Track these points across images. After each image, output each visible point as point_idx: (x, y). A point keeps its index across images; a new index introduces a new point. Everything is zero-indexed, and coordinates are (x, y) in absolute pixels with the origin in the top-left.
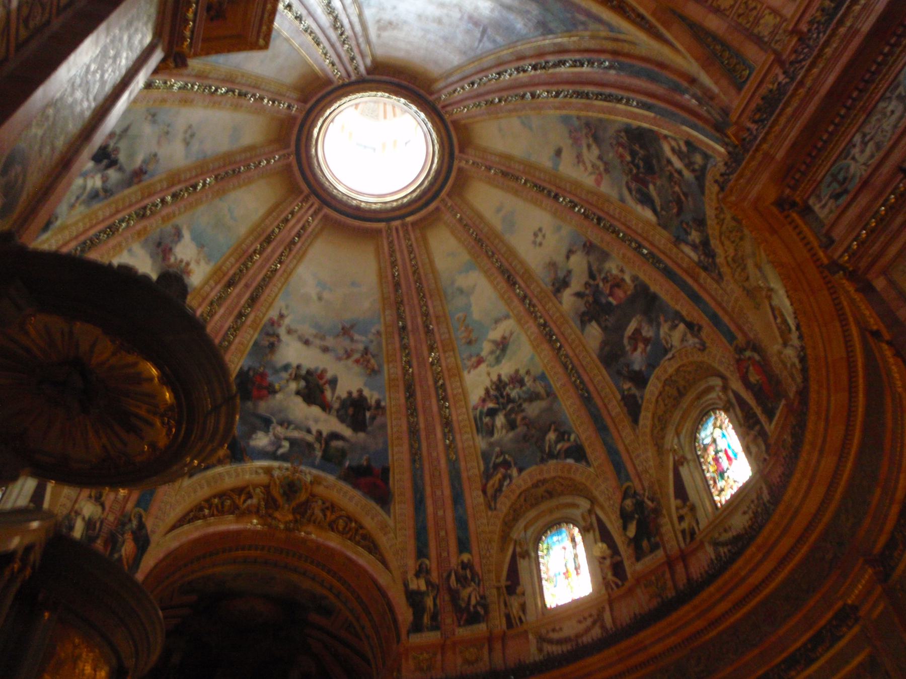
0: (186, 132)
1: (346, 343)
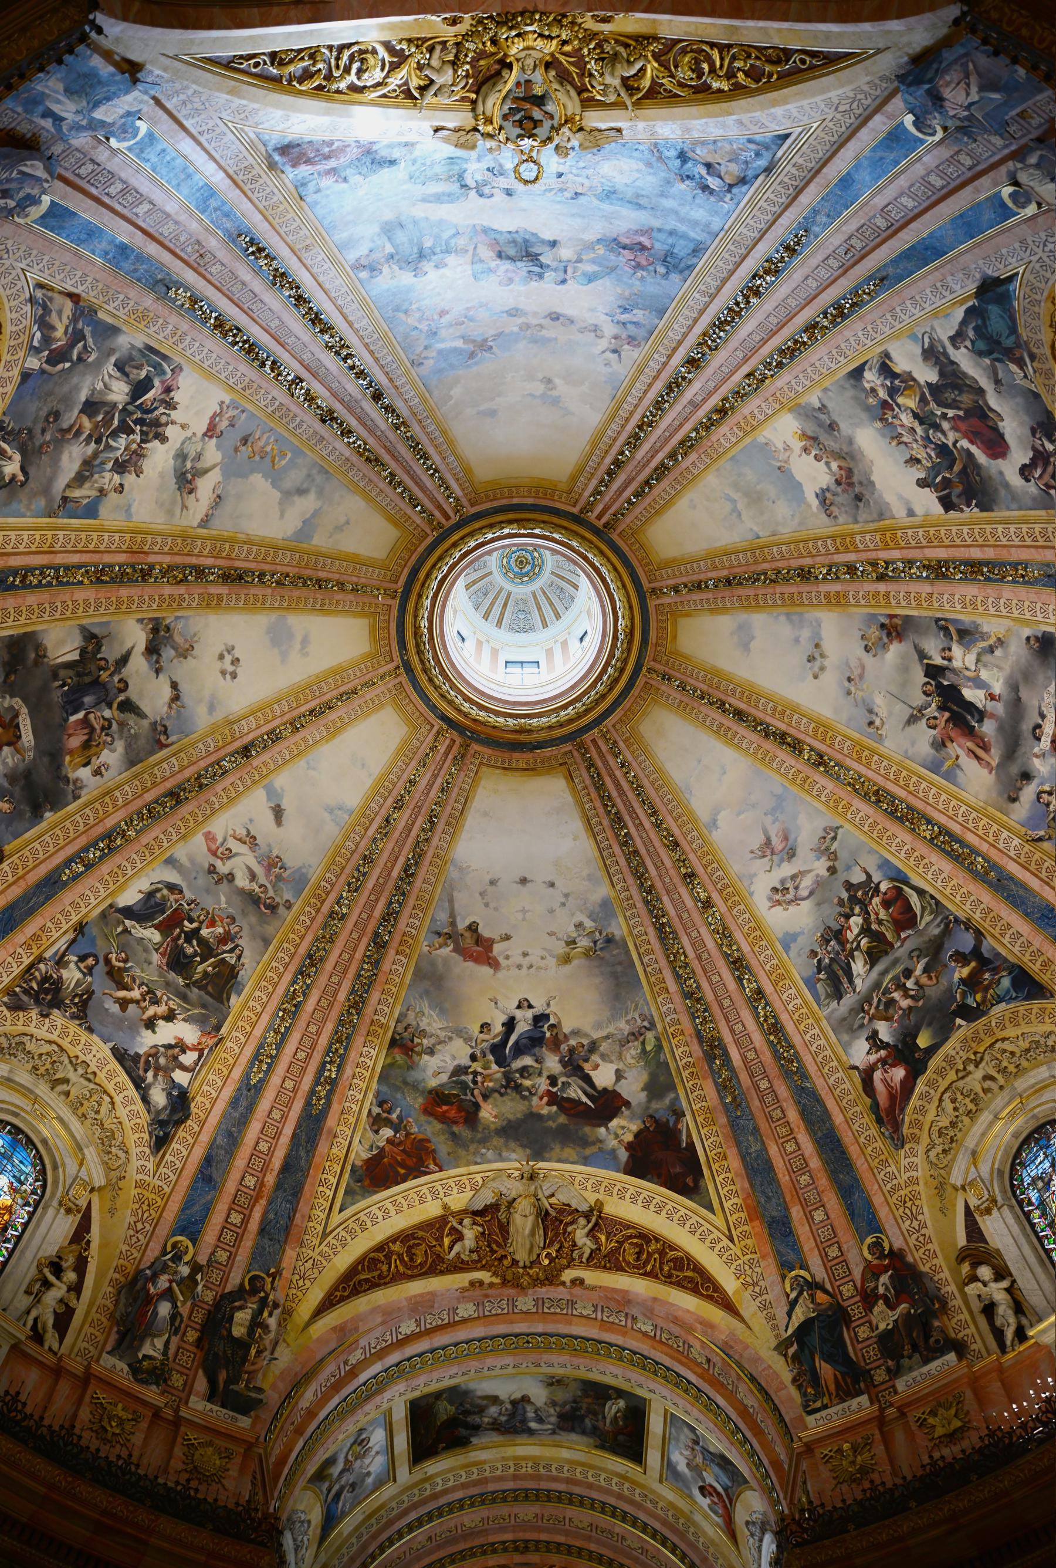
0: (822, 668)
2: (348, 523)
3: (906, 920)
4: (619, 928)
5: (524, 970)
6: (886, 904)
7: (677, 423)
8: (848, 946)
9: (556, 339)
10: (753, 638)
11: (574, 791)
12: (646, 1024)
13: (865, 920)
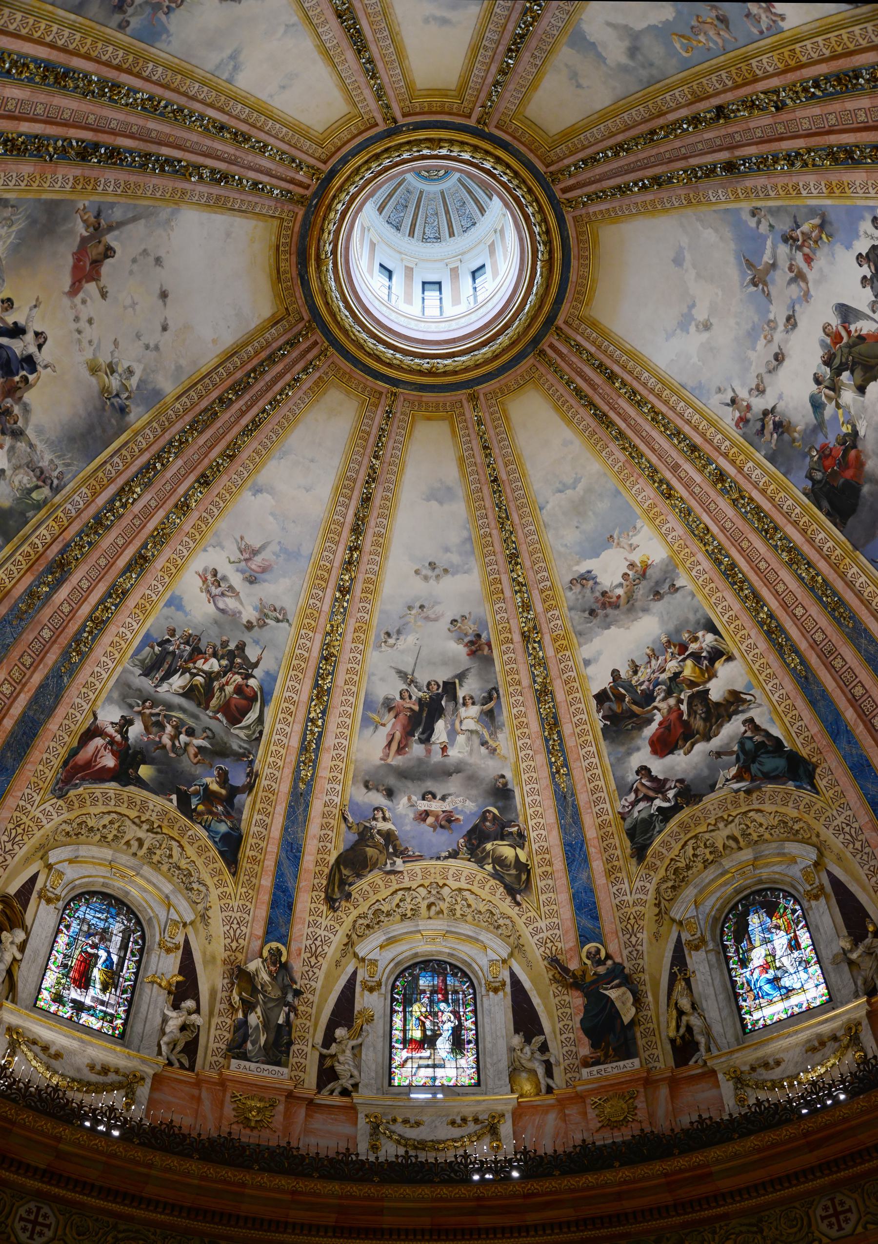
0: (426, 578)
1: (781, 276)
2: (579, 86)
3: (234, 715)
4: (138, 417)
5: (74, 326)
6: (239, 690)
7: (656, 447)
8: (191, 665)
9: (754, 349)
10: (441, 503)
11: (261, 330)
12: (56, 482)
13: (218, 672)
